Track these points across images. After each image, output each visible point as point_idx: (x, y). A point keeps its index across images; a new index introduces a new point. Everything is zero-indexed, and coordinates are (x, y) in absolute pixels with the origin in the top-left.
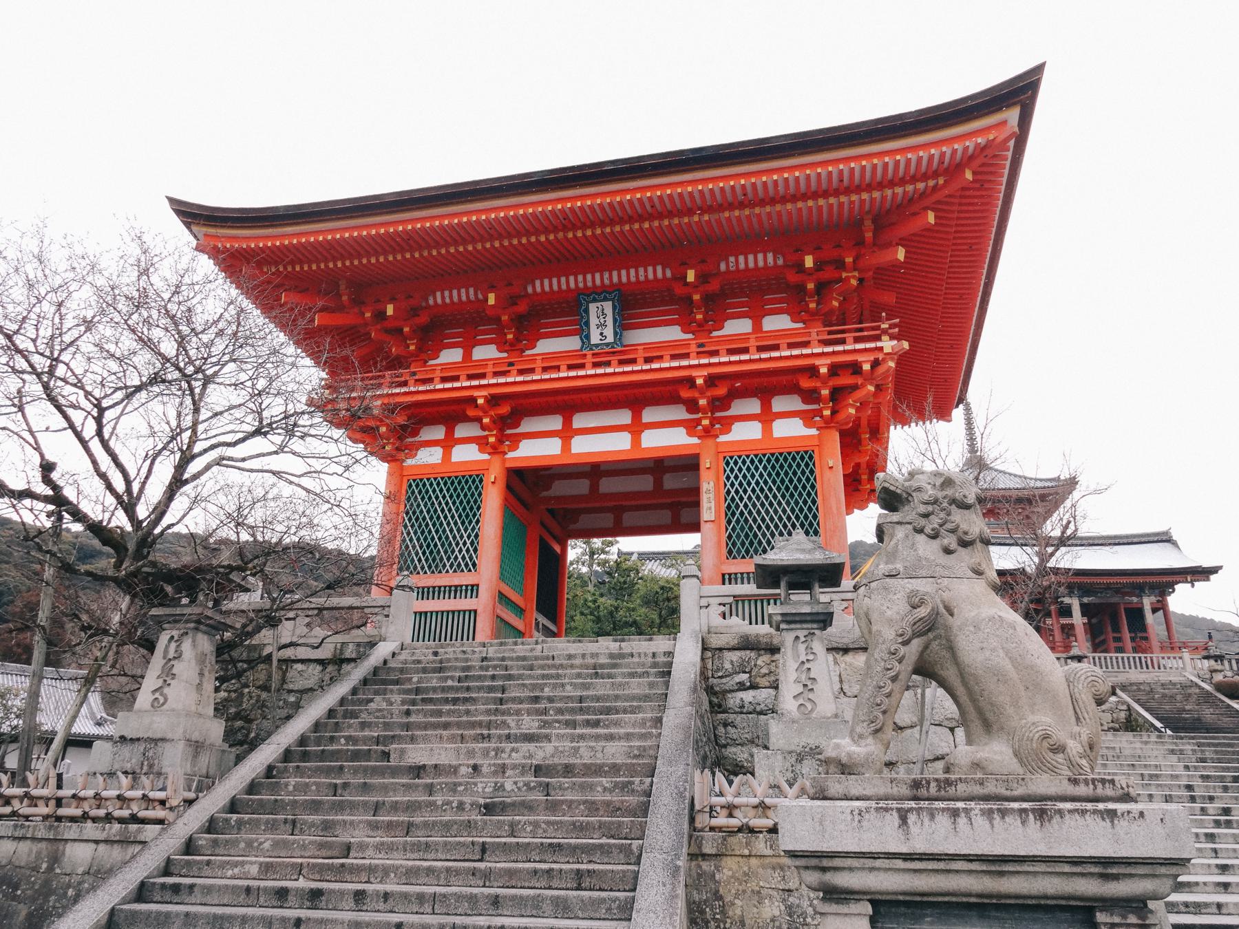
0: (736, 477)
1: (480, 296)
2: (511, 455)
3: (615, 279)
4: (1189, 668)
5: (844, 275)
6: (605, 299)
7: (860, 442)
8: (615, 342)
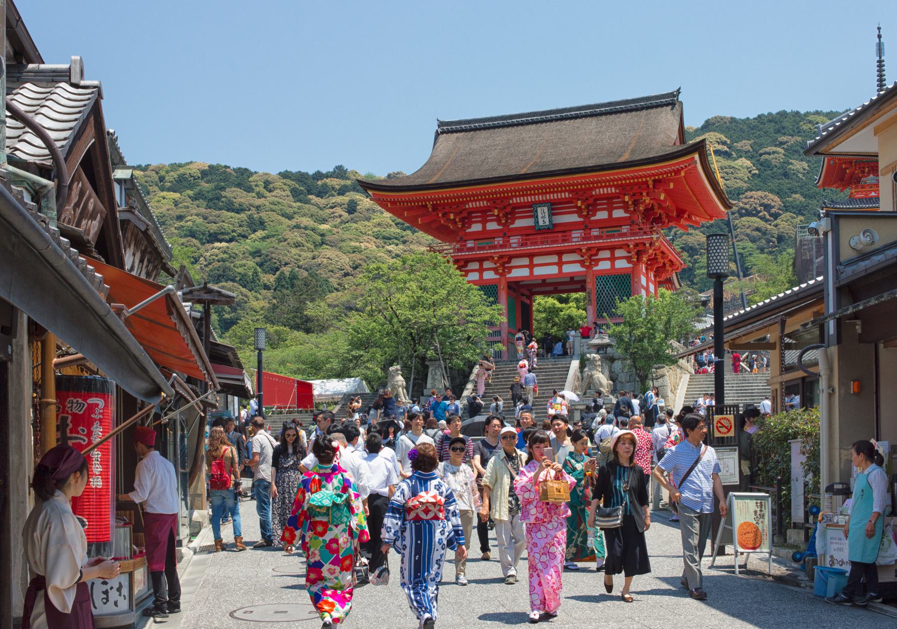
2: (508, 276)
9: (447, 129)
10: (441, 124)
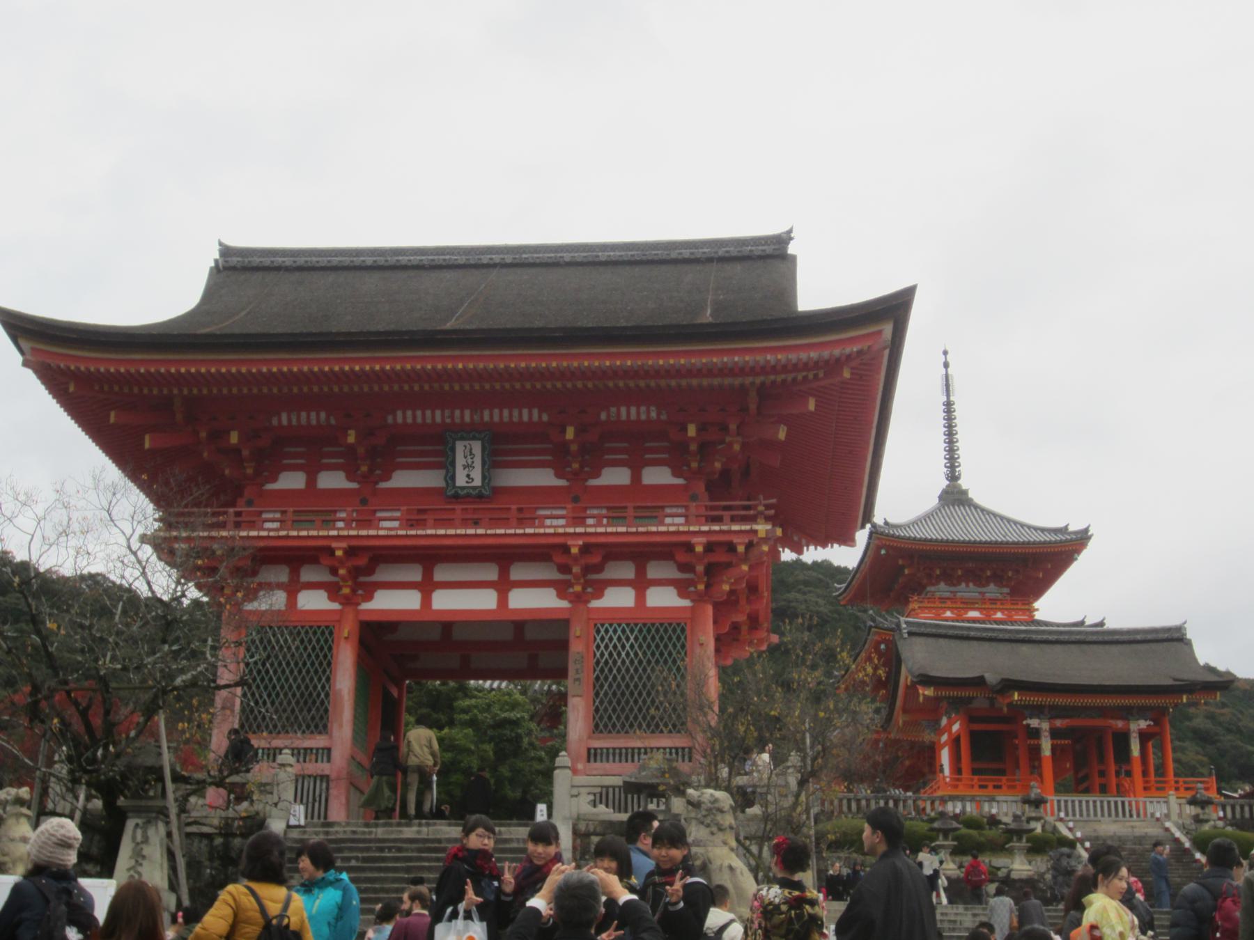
0: (606, 647)
1: (333, 422)
2: (365, 606)
3: (486, 418)
4: (1174, 817)
5: (728, 439)
6: (474, 438)
7: (737, 601)
8: (483, 486)
9: (236, 268)
10: (226, 251)
